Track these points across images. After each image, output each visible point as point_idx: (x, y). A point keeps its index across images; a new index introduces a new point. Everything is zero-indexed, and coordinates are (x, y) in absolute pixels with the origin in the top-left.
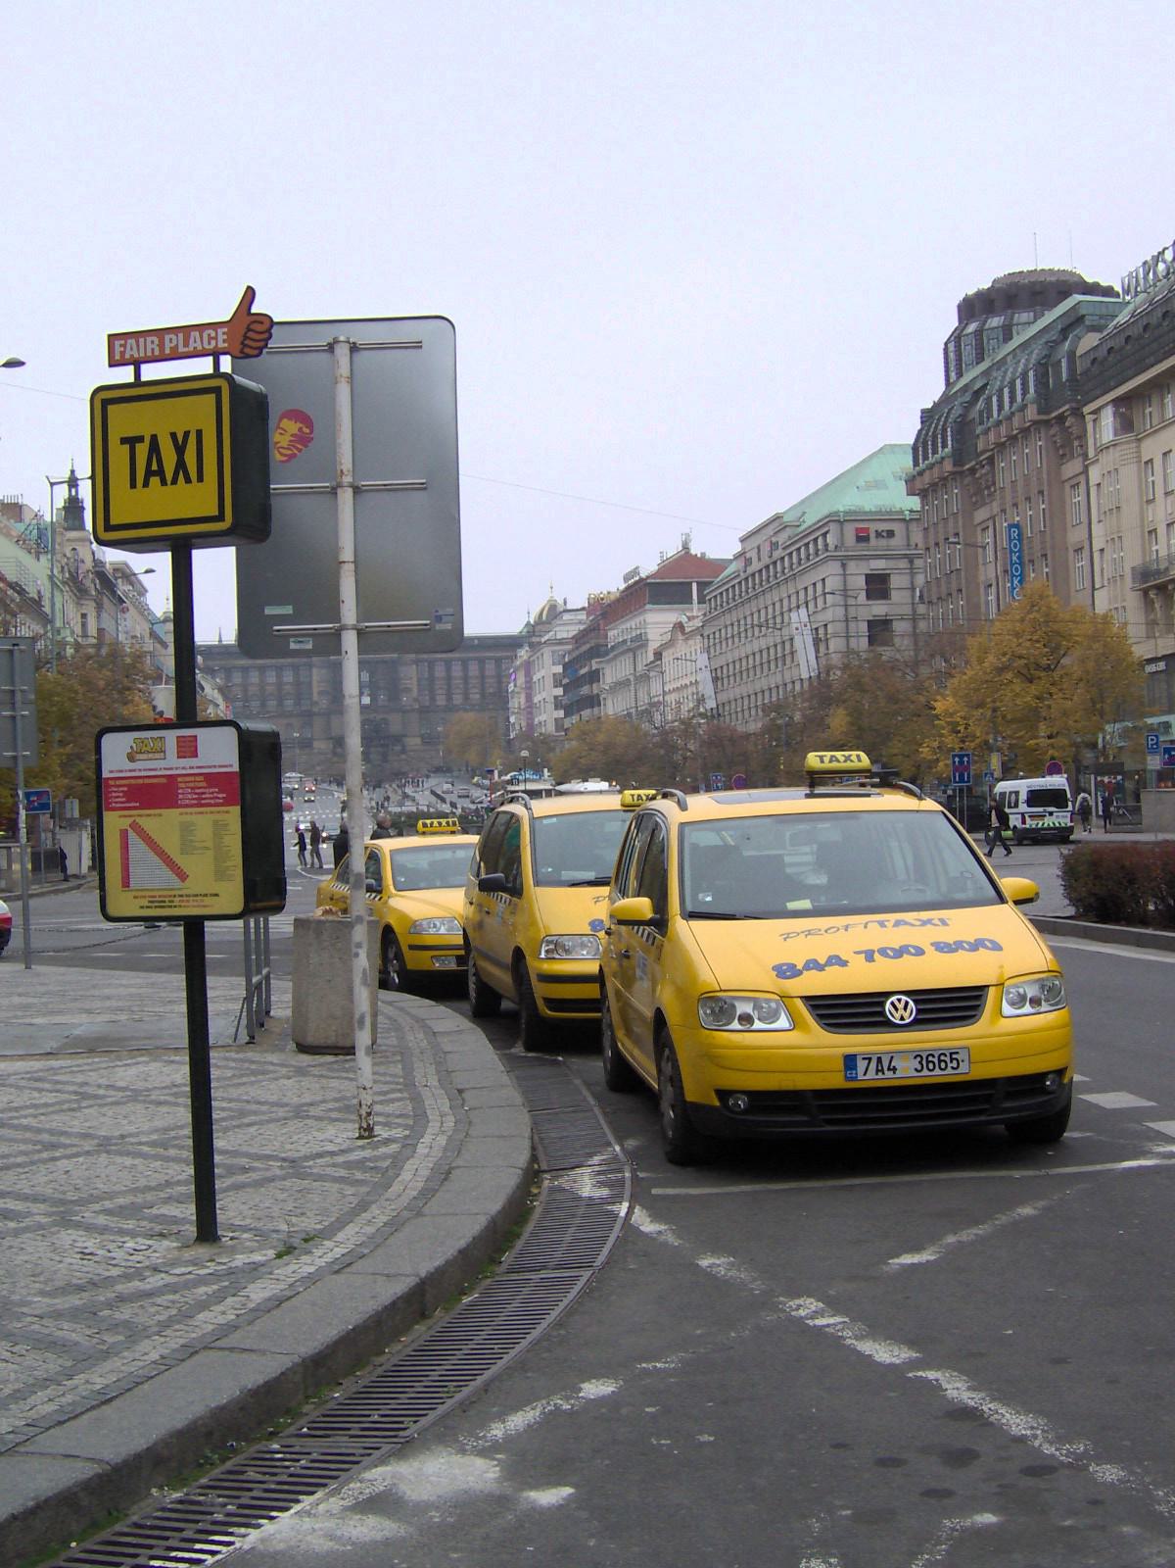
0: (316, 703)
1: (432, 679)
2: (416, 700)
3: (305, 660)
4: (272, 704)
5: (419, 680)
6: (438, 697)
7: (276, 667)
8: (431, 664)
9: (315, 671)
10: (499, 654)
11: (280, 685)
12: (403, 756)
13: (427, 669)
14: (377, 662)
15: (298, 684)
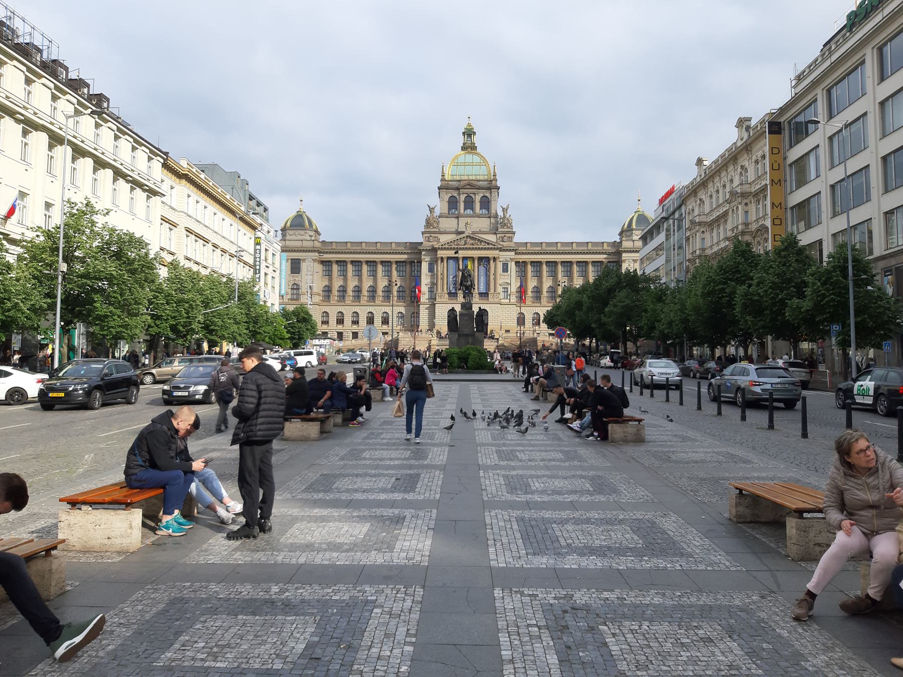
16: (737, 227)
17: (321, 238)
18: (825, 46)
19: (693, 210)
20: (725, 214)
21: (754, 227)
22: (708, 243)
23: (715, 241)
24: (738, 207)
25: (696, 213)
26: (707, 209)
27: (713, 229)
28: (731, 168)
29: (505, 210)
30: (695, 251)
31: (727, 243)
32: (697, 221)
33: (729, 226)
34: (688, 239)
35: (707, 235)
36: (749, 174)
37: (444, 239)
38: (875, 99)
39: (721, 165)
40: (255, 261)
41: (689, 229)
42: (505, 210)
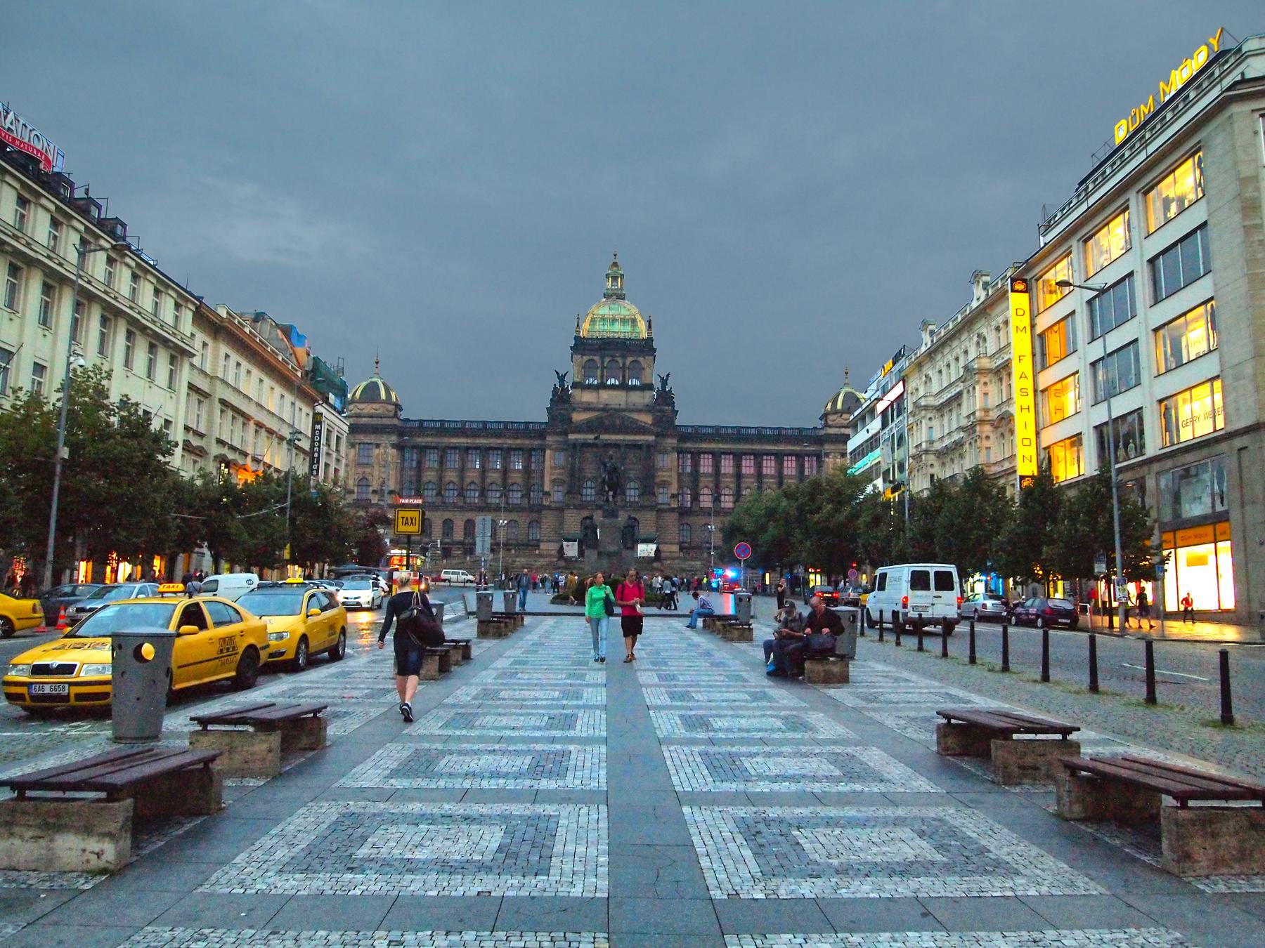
0: (547, 494)
1: (695, 474)
2: (673, 496)
3: (537, 442)
4: (494, 498)
5: (679, 475)
6: (701, 498)
7: (500, 449)
8: (696, 455)
9: (548, 452)
10: (782, 447)
11: (505, 472)
12: (655, 565)
13: (689, 461)
14: (627, 446)
15: (527, 470)
16: (974, 413)
17: (403, 415)
18: (1081, 184)
19: (917, 390)
20: (959, 395)
21: (994, 415)
22: (937, 434)
23: (946, 431)
24: (974, 388)
25: (921, 393)
26: (935, 388)
27: (942, 416)
28: (965, 336)
29: (664, 382)
30: (921, 444)
31: (962, 434)
32: (923, 404)
33: (965, 411)
34: (910, 430)
35: (935, 423)
36: (988, 345)
37: (578, 417)
38: (1142, 256)
39: (953, 332)
40: (312, 446)
41: (913, 414)
42: (664, 382)
